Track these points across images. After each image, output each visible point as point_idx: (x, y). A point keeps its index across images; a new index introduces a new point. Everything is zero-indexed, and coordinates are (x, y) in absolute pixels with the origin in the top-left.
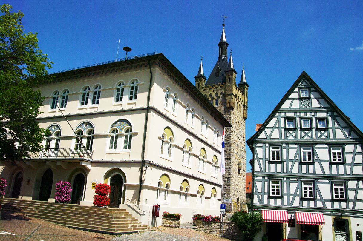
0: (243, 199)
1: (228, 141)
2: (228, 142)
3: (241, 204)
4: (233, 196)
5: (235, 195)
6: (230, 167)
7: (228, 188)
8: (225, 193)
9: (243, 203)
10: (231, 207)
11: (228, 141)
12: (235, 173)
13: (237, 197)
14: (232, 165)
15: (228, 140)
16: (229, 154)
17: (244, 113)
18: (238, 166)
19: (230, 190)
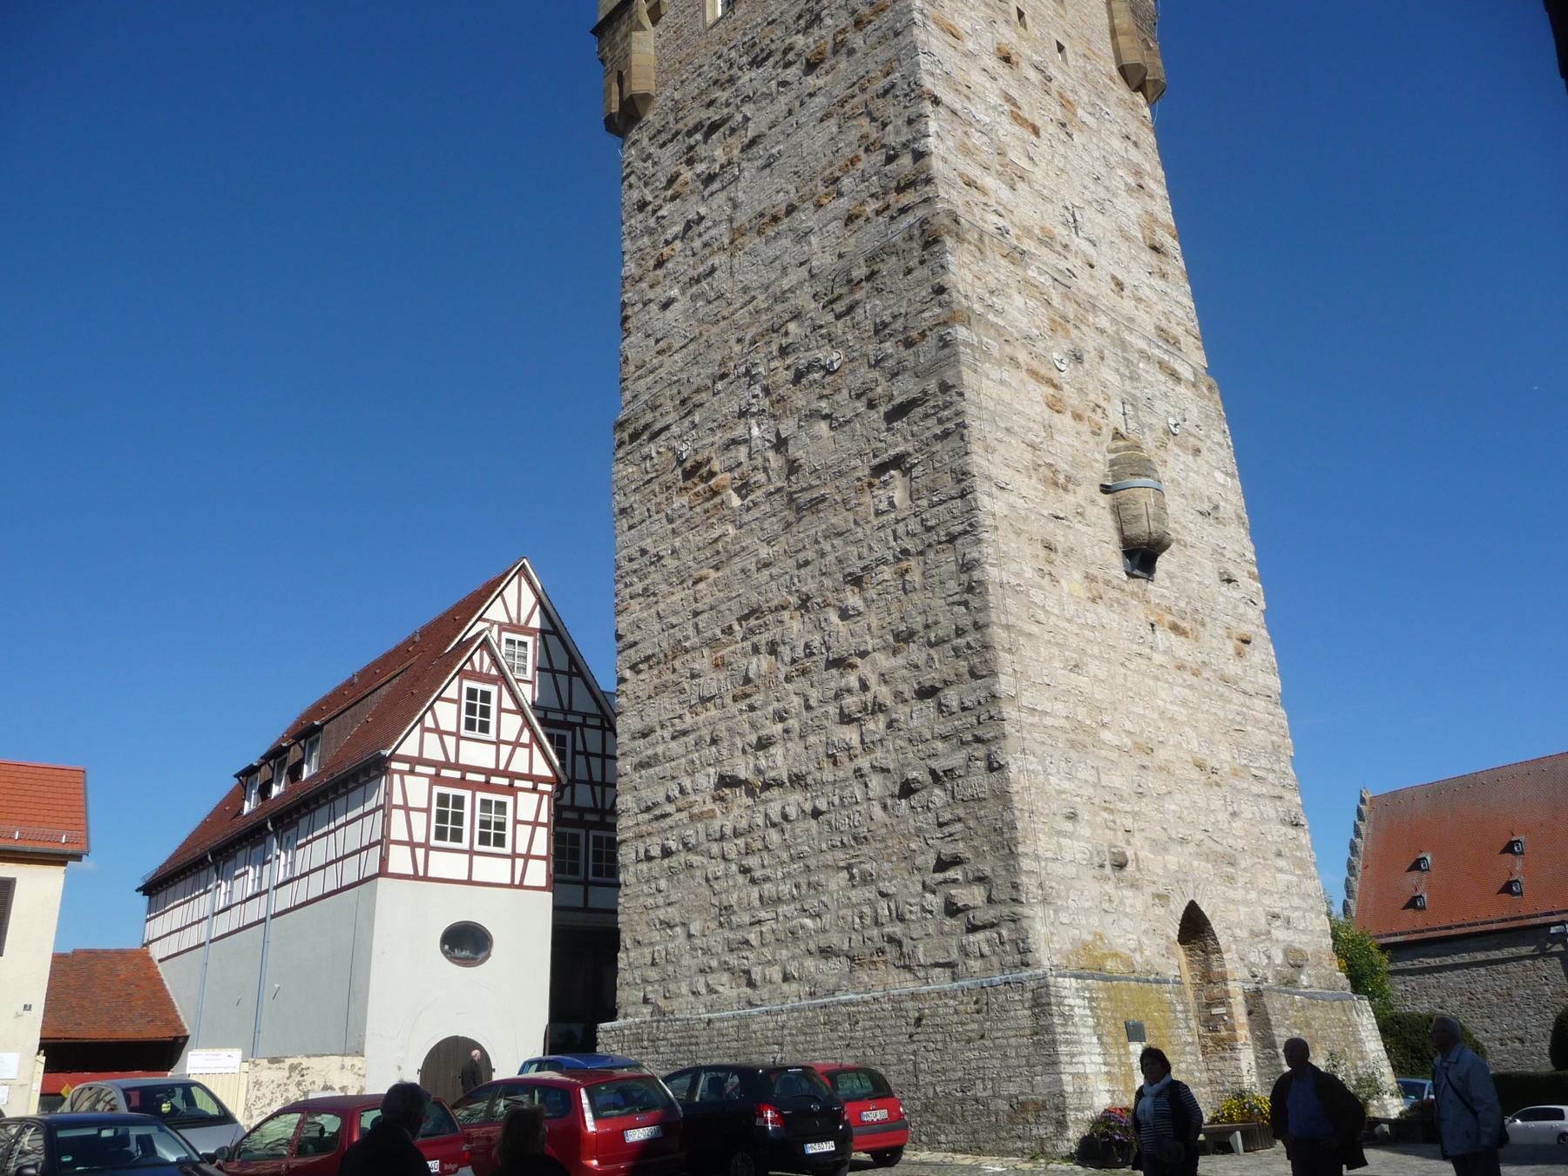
0: (1280, 934)
1: (904, 210)
2: (910, 219)
3: (1255, 999)
4: (1090, 890)
5: (1121, 866)
6: (962, 496)
7: (979, 781)
8: (956, 861)
9: (1290, 983)
10: (1052, 1063)
11: (904, 210)
12: (1072, 583)
13: (1162, 898)
14: (1003, 475)
15: (908, 198)
16: (932, 339)
17: (1114, 32)
18: (1117, 510)
19: (1003, 796)
